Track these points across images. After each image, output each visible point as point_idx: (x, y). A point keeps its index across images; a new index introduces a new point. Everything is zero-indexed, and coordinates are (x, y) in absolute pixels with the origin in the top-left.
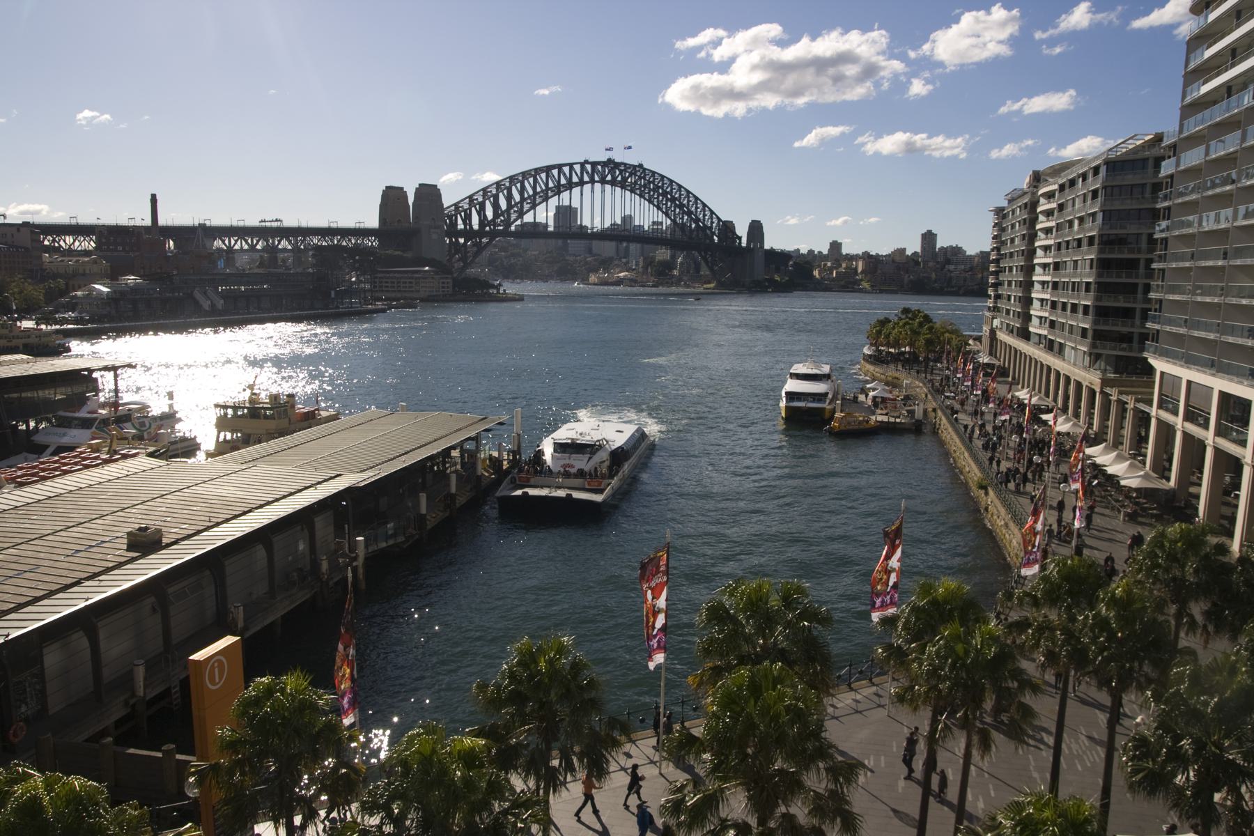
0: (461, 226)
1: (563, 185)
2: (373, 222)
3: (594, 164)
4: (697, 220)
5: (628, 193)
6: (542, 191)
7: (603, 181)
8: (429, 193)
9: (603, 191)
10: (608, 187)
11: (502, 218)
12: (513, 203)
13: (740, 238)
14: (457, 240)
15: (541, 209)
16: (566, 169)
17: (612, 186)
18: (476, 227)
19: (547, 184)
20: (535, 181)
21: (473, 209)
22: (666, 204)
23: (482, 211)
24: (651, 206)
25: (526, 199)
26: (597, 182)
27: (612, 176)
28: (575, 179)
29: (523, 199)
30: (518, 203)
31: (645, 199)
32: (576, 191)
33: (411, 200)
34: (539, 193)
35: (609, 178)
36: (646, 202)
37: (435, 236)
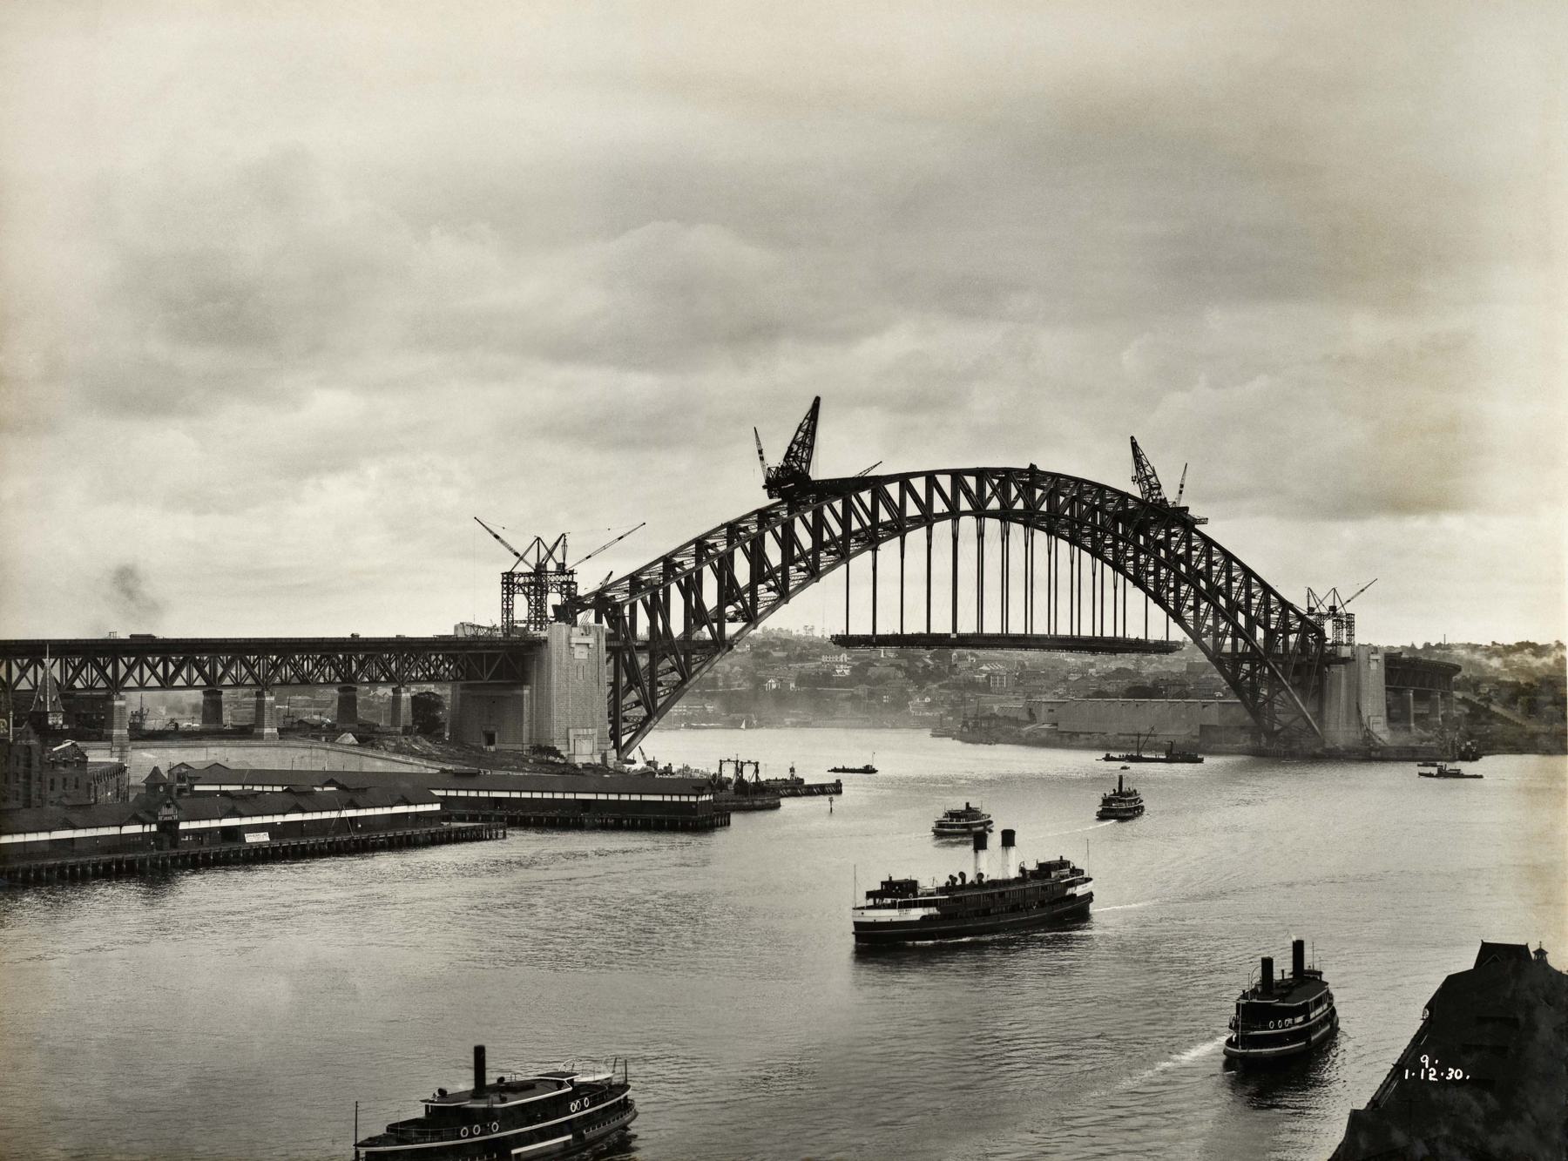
5: (1064, 546)
7: (1006, 515)
9: (1005, 534)
10: (1017, 529)
12: (796, 552)
17: (1026, 525)
19: (873, 515)
20: (848, 507)
22: (1156, 573)
24: (1121, 577)
26: (993, 514)
30: (809, 552)
31: (1105, 560)
34: (857, 532)
35: (1020, 505)
36: (1108, 569)
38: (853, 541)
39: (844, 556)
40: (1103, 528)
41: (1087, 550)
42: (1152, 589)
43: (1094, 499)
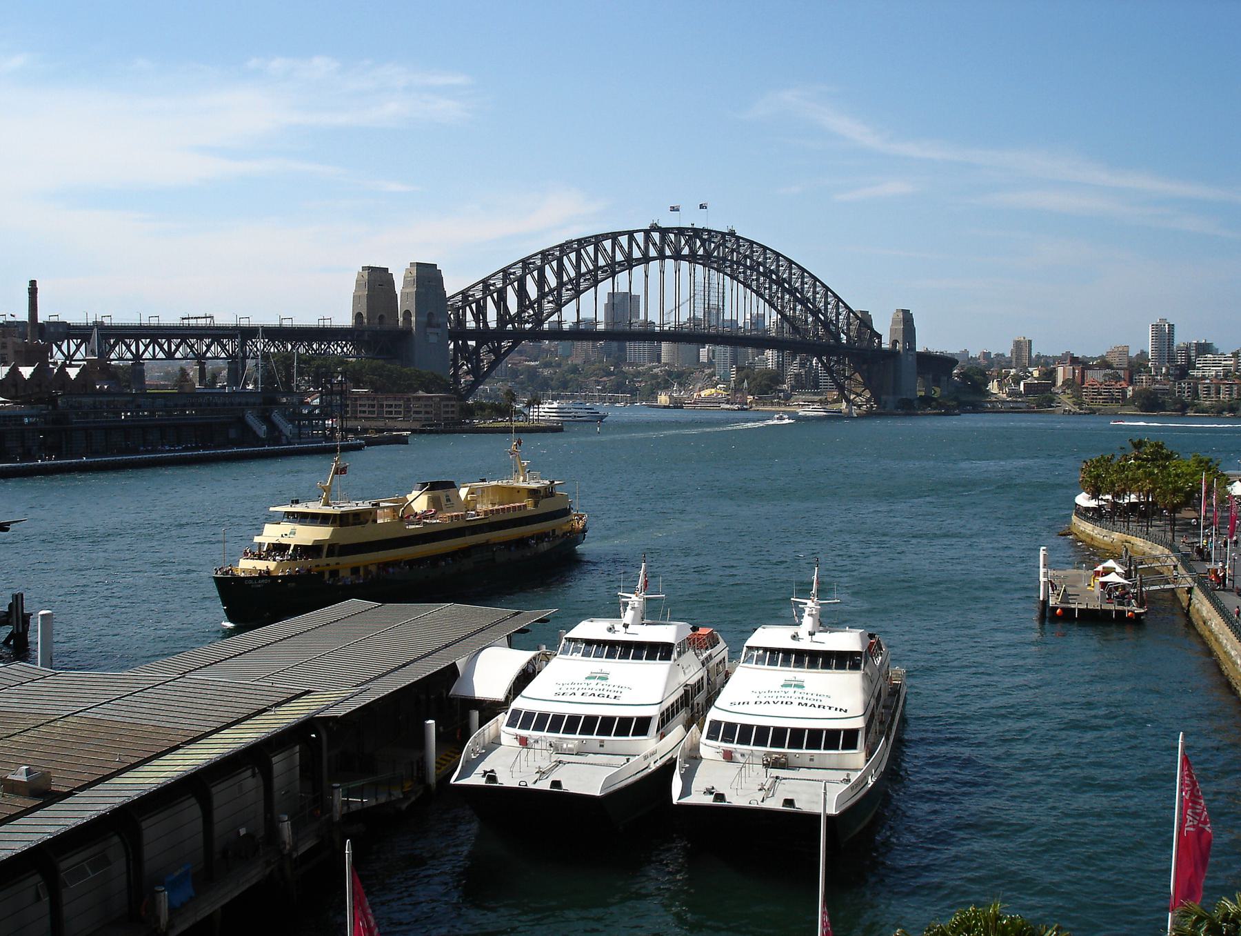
0: (471, 324)
1: (619, 263)
2: (345, 319)
3: (664, 232)
4: (815, 313)
6: (589, 272)
7: (677, 256)
8: (427, 276)
9: (678, 270)
10: (685, 265)
11: (531, 312)
12: (547, 289)
13: (879, 337)
14: (465, 343)
15: (587, 297)
16: (624, 240)
18: (493, 325)
20: (579, 258)
21: (489, 298)
22: (770, 289)
23: (501, 302)
25: (566, 284)
26: (669, 257)
27: (690, 248)
28: (637, 254)
29: (561, 284)
31: (739, 281)
32: (638, 270)
33: (399, 287)
34: (584, 275)
35: (686, 251)
36: (741, 286)
37: (433, 339)
38: (582, 280)
39: (577, 294)
40: (738, 263)
41: (728, 275)
42: (768, 298)
43: (733, 245)
